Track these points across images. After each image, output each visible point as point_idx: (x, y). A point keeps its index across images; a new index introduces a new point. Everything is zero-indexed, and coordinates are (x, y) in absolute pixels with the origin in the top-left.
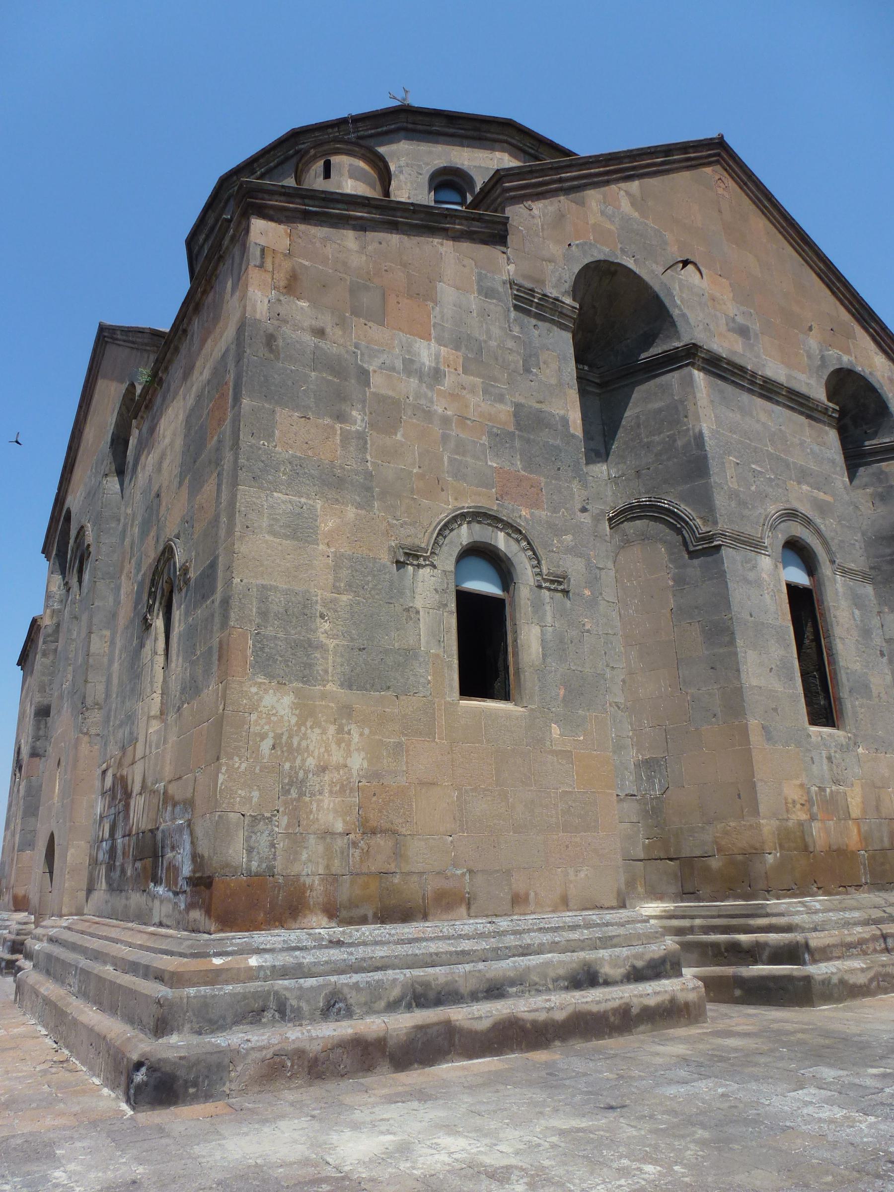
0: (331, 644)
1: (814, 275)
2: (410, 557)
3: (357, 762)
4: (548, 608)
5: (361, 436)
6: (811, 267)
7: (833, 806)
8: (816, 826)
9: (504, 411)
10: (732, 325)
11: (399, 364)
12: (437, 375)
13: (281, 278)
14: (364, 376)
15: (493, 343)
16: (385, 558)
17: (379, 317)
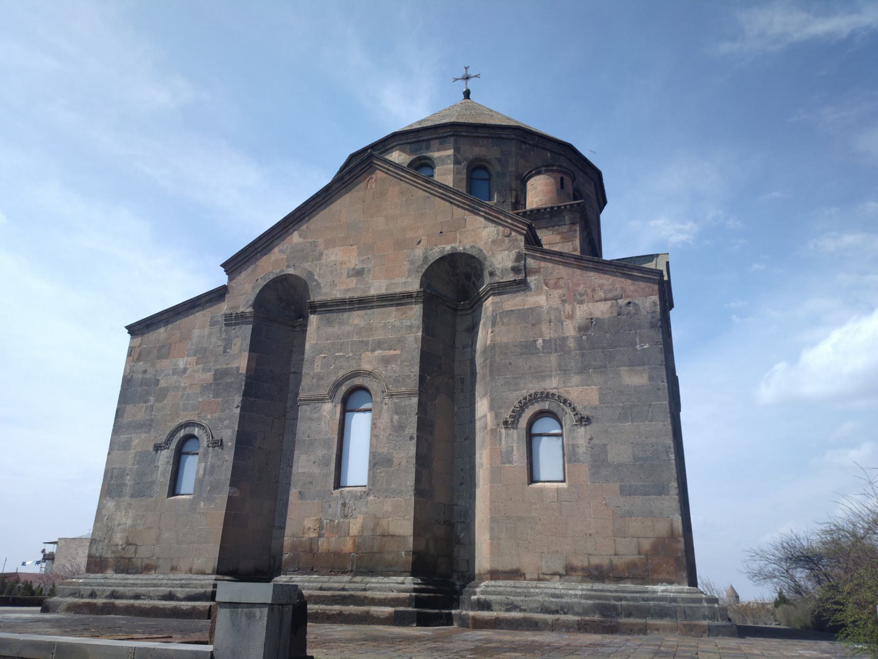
0: (129, 483)
1: (436, 198)
2: (158, 448)
3: (129, 522)
4: (210, 455)
5: (152, 406)
6: (435, 195)
7: (339, 530)
8: (321, 540)
9: (209, 376)
10: (351, 272)
11: (171, 372)
12: (185, 370)
13: (136, 356)
14: (157, 382)
15: (211, 346)
16: (151, 449)
17: (166, 356)
